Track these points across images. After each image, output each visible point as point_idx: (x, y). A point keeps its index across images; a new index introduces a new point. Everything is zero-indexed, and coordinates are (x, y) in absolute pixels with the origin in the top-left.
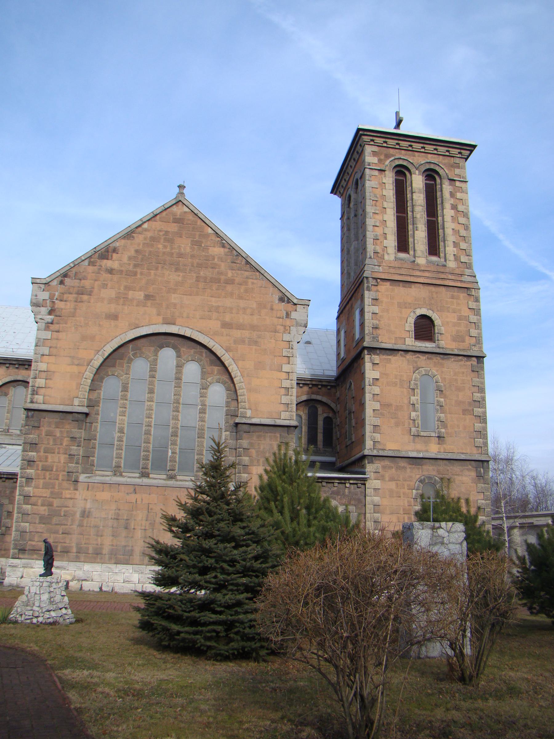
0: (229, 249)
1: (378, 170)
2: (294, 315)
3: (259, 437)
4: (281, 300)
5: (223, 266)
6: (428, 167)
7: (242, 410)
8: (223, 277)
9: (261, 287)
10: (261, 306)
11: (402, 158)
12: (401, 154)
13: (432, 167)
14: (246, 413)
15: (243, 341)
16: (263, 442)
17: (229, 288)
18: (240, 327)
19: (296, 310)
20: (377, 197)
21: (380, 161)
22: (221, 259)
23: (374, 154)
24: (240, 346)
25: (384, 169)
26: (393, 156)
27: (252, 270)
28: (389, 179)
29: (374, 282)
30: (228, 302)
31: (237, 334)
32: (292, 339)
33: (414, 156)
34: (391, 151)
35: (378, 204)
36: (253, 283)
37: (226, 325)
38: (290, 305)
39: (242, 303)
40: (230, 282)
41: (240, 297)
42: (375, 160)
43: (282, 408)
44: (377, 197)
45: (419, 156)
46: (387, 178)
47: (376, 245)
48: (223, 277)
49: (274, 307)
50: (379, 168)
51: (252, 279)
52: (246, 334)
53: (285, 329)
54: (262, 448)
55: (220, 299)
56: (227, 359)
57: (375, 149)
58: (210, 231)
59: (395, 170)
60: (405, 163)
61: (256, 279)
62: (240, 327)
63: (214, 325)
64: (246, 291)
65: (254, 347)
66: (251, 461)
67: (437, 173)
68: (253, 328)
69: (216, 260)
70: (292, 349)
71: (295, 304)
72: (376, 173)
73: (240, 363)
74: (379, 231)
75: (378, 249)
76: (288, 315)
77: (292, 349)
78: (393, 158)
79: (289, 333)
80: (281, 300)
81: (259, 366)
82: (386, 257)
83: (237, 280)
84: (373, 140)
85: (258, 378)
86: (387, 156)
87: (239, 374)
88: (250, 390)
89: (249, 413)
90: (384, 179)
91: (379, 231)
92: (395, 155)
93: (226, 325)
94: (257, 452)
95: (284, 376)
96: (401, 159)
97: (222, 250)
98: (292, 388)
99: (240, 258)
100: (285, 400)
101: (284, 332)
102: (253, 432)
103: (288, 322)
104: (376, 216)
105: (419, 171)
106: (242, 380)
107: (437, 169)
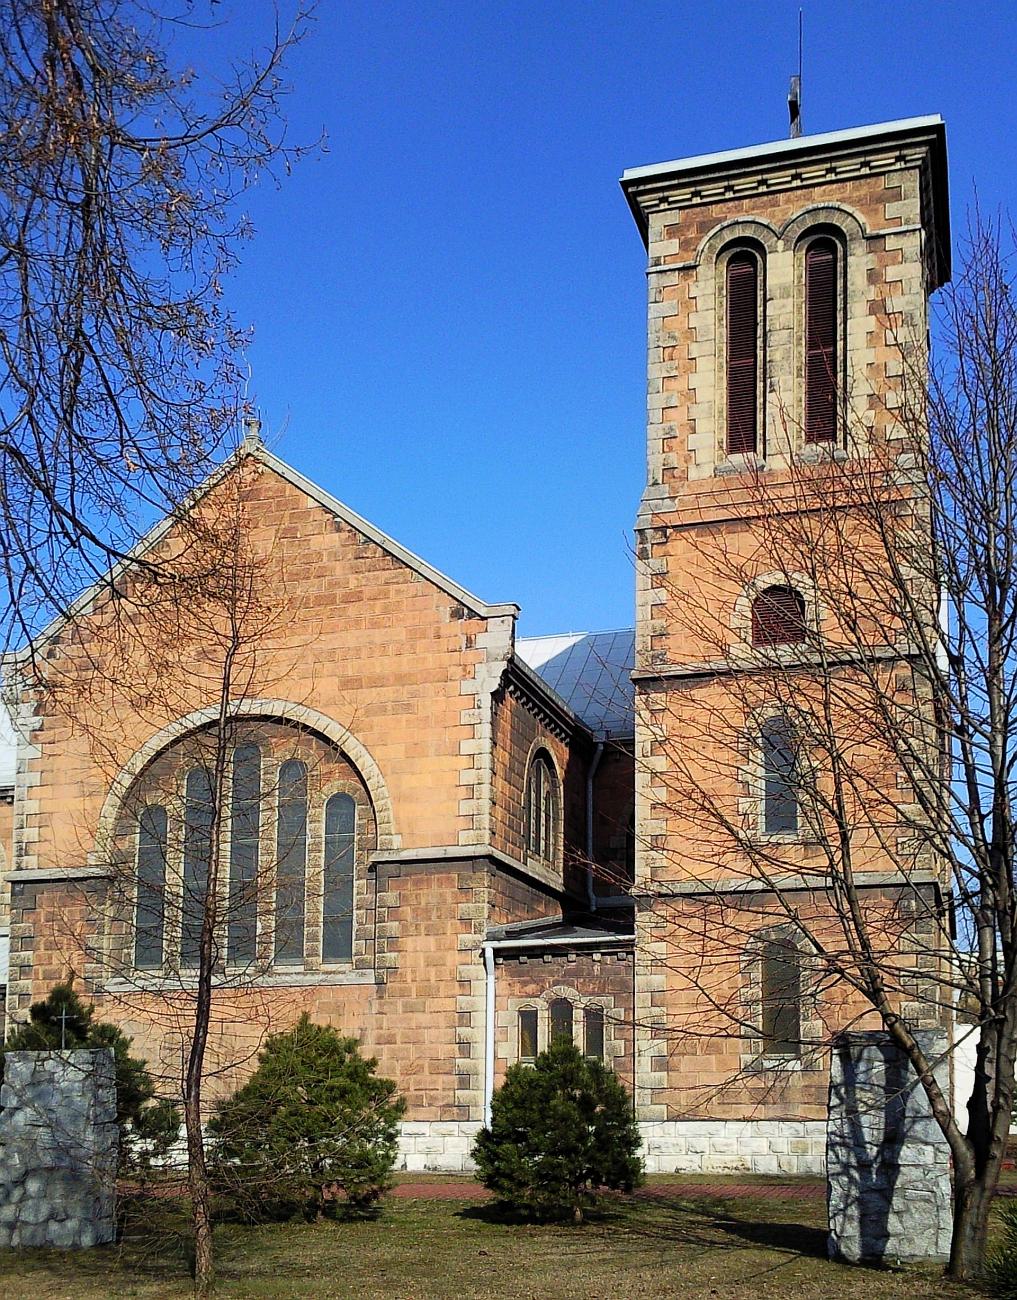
0: (350, 531)
1: (679, 269)
2: (481, 641)
3: (416, 883)
4: (456, 614)
5: (339, 569)
6: (810, 222)
7: (384, 837)
8: (339, 592)
9: (416, 596)
10: (416, 634)
11: (740, 220)
12: (739, 210)
13: (822, 219)
14: (391, 842)
15: (383, 710)
16: (425, 891)
17: (352, 610)
18: (377, 682)
19: (486, 631)
20: (674, 338)
21: (685, 245)
22: (334, 556)
23: (672, 230)
24: (376, 719)
25: (692, 263)
26: (719, 221)
27: (397, 565)
28: (710, 286)
29: (658, 537)
30: (351, 638)
31: (369, 695)
32: (479, 689)
33: (776, 204)
34: (715, 211)
35: (676, 354)
36: (398, 592)
37: (348, 683)
38: (474, 621)
39: (378, 636)
40: (354, 597)
41: (375, 625)
42: (673, 246)
43: (462, 823)
44: (674, 338)
45: (788, 201)
46: (701, 284)
47: (671, 449)
48: (339, 592)
49: (443, 632)
50: (681, 265)
51: (398, 583)
52: (388, 693)
53: (465, 670)
54: (423, 903)
55: (336, 635)
56: (353, 748)
57: (674, 217)
58: (311, 503)
59: (727, 256)
60: (749, 233)
61: (406, 582)
62: (377, 682)
63: (328, 686)
64: (386, 611)
65: (405, 717)
66: (405, 928)
67: (836, 231)
68: (401, 679)
69: (325, 559)
70: (479, 707)
71: (483, 619)
72: (675, 278)
73: (378, 752)
74: (677, 418)
75: (674, 459)
76: (470, 643)
77: (479, 707)
78: (718, 228)
79: (474, 678)
80: (456, 614)
81: (415, 750)
82: (693, 474)
83: (367, 592)
84: (663, 200)
85: (413, 774)
86: (703, 228)
87: (377, 771)
88: (398, 799)
89: (397, 842)
90: (692, 288)
91: (677, 418)
92: (725, 218)
93: (348, 683)
94: (414, 911)
95: (464, 762)
96: (737, 223)
97: (336, 535)
98: (479, 784)
99: (372, 545)
100: (466, 808)
101: (464, 677)
102: (406, 875)
103: (470, 656)
104: (673, 384)
105: (787, 242)
106: (382, 782)
107: (836, 220)
